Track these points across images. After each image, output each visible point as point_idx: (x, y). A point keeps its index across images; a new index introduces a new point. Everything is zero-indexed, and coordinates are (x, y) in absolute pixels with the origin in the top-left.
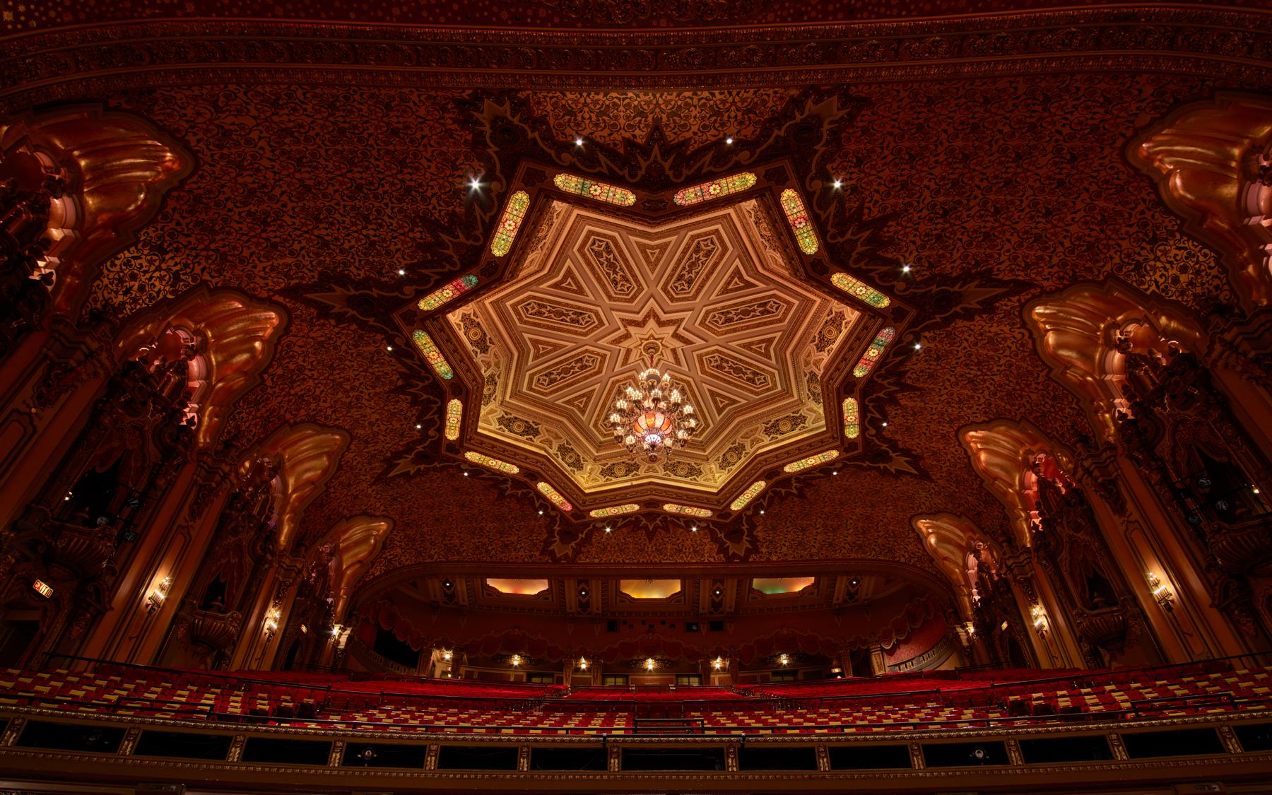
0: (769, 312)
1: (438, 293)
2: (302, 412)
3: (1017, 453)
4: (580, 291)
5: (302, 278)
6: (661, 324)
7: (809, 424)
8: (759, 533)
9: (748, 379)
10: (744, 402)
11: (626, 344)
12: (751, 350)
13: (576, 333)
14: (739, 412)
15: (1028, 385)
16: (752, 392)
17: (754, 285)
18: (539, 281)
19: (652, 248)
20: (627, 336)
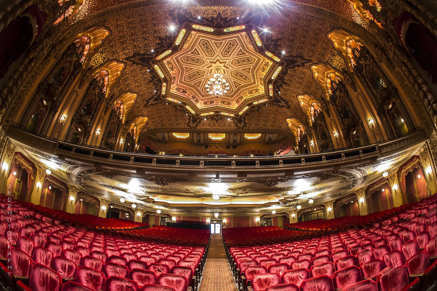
1: (161, 55)
2: (128, 89)
3: (309, 102)
4: (198, 54)
5: (130, 55)
6: (220, 63)
7: (260, 91)
8: (246, 121)
9: (244, 79)
10: (243, 85)
11: (211, 68)
12: (245, 71)
13: (197, 65)
15: (312, 85)
16: (245, 82)
17: (245, 54)
18: (188, 52)
19: (218, 43)
20: (211, 66)
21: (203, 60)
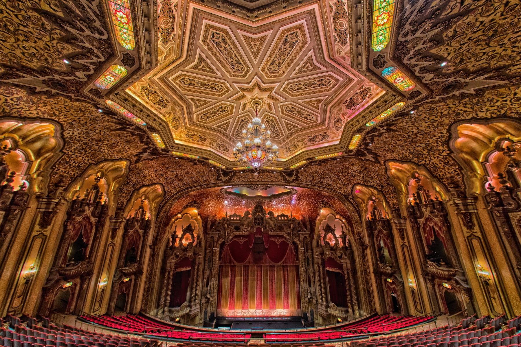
6: (263, 90)
10: (300, 127)
11: (243, 101)
14: (297, 131)
16: (306, 123)
19: (254, 40)
20: (243, 97)
21: (224, 84)
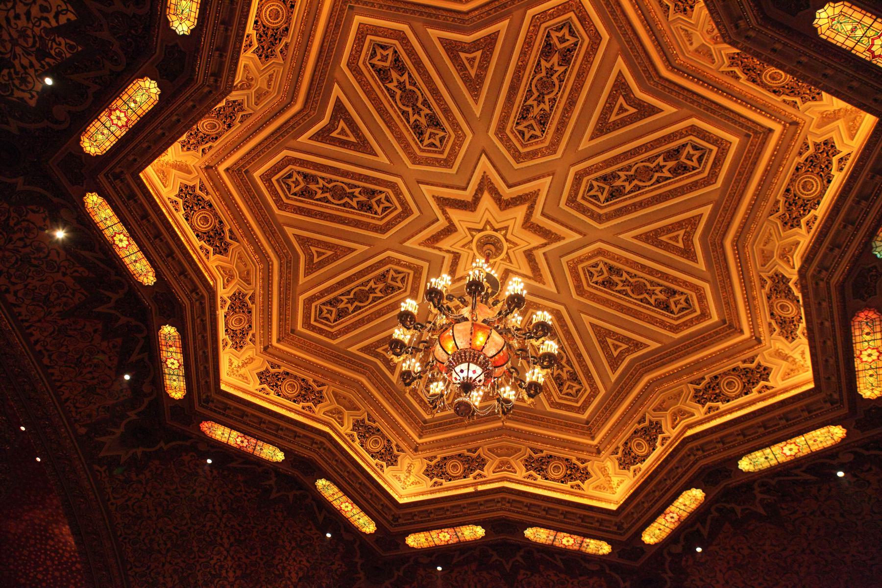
0: (685, 168)
7: (776, 381)
10: (654, 345)
20: (450, 229)
